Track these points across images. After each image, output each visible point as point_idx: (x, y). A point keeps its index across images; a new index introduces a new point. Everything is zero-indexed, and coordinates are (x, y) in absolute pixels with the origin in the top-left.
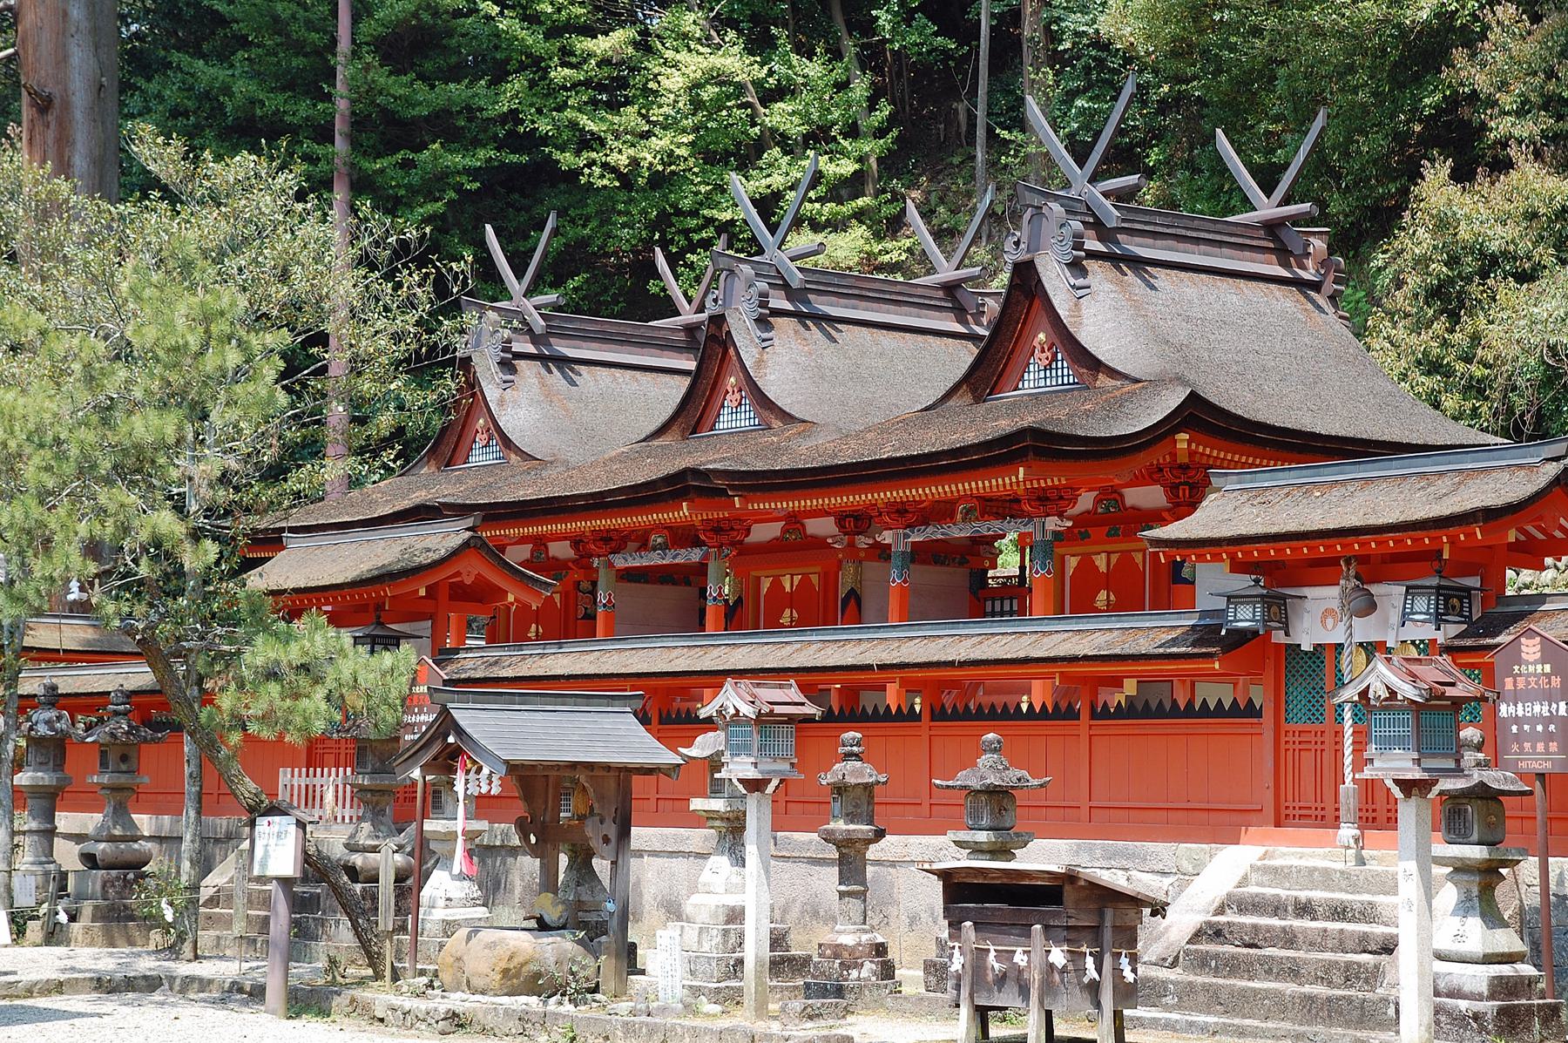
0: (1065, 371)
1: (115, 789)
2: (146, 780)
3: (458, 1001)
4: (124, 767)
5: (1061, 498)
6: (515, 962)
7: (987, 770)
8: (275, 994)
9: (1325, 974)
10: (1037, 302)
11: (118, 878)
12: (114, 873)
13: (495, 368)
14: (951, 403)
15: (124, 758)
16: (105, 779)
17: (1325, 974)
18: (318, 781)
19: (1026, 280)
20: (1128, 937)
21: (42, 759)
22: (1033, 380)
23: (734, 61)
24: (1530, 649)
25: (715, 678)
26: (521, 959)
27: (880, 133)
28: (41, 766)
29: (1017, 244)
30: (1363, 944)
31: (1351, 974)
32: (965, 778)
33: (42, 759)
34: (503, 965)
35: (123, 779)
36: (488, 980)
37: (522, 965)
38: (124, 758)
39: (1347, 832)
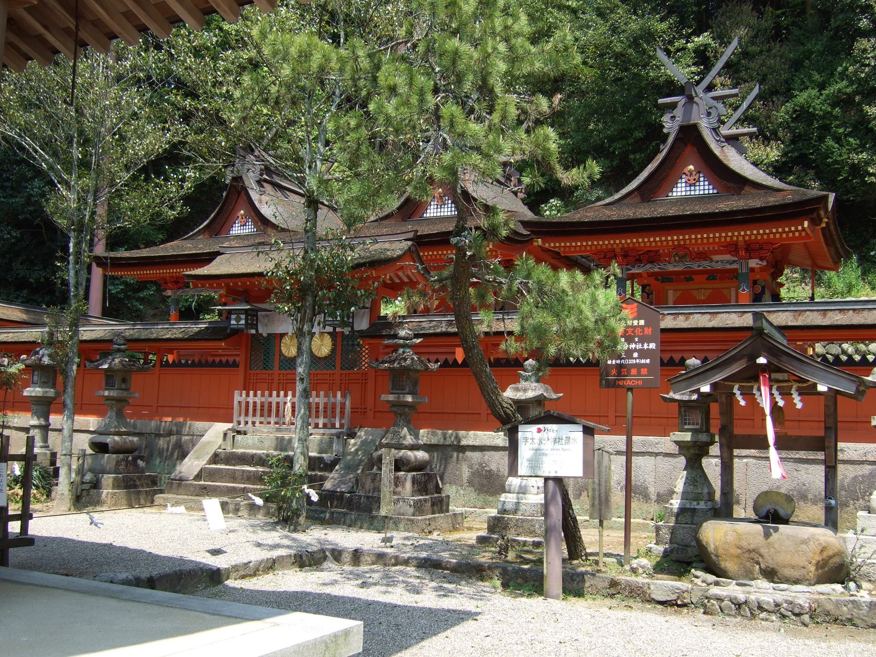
0: (704, 188)
1: (119, 400)
2: (137, 395)
4: (124, 386)
5: (761, 249)
6: (825, 554)
11: (123, 460)
12: (121, 456)
13: (254, 185)
14: (625, 201)
15: (124, 380)
16: (113, 393)
18: (281, 399)
21: (46, 380)
22: (680, 190)
26: (831, 553)
28: (43, 384)
29: (673, 118)
33: (46, 380)
34: (818, 558)
35: (125, 394)
36: (804, 572)
37: (831, 557)
38: (124, 380)
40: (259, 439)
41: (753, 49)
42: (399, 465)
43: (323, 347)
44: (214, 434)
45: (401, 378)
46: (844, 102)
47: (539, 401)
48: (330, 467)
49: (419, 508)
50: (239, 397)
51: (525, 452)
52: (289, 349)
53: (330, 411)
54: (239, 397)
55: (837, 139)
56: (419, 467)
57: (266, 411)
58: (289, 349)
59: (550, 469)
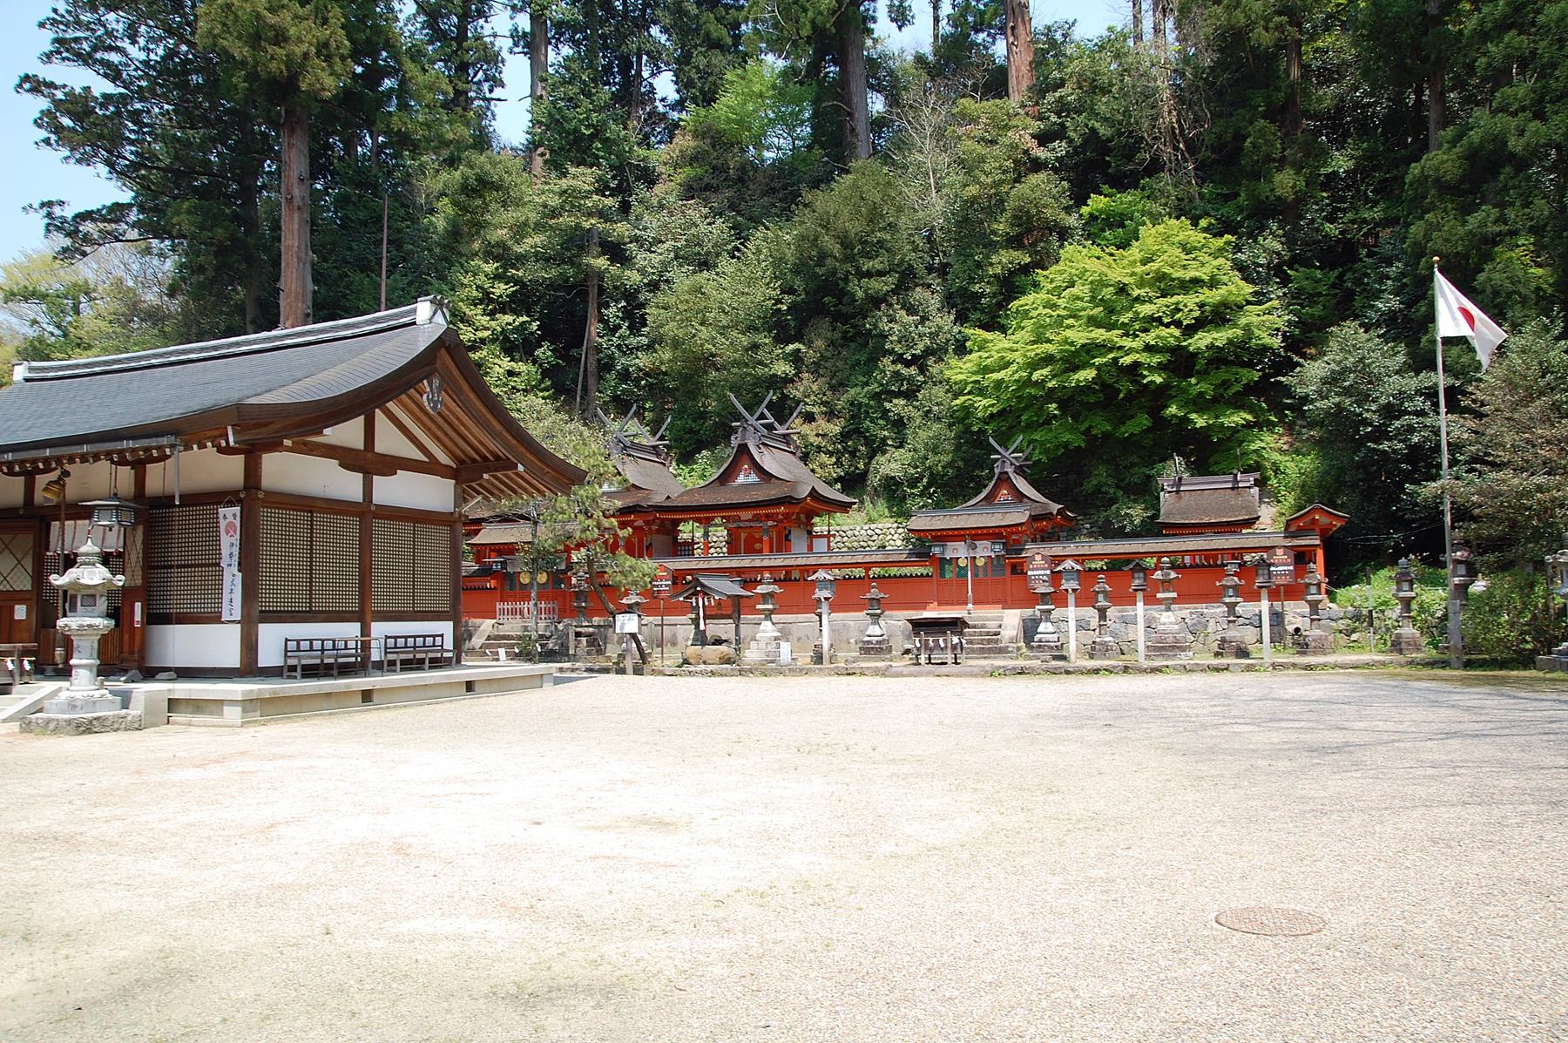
0: (753, 478)
3: (710, 668)
7: (874, 593)
8: (630, 669)
9: (982, 642)
10: (745, 457)
17: (982, 642)
19: (743, 449)
20: (961, 634)
22: (741, 479)
23: (506, 364)
24: (1038, 558)
25: (814, 568)
27: (546, 389)
30: (988, 634)
31: (989, 641)
32: (868, 596)
39: (970, 606)
40: (512, 626)
41: (828, 354)
42: (578, 634)
43: (542, 578)
44: (486, 626)
45: (579, 595)
46: (876, 396)
47: (637, 604)
48: (548, 638)
49: (589, 653)
50: (499, 606)
51: (618, 624)
52: (525, 579)
53: (548, 611)
54: (499, 606)
55: (872, 421)
56: (588, 635)
57: (514, 612)
58: (525, 579)
59: (627, 630)
